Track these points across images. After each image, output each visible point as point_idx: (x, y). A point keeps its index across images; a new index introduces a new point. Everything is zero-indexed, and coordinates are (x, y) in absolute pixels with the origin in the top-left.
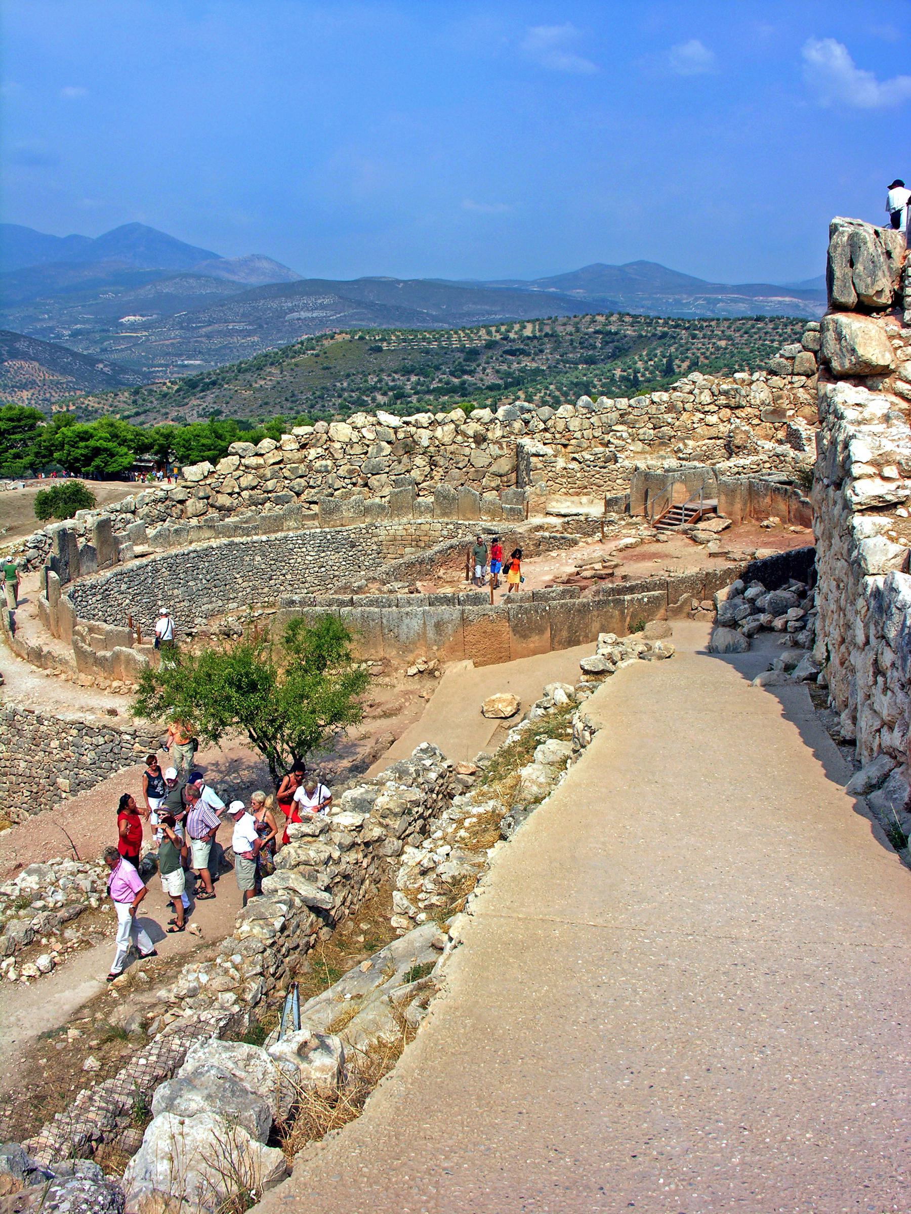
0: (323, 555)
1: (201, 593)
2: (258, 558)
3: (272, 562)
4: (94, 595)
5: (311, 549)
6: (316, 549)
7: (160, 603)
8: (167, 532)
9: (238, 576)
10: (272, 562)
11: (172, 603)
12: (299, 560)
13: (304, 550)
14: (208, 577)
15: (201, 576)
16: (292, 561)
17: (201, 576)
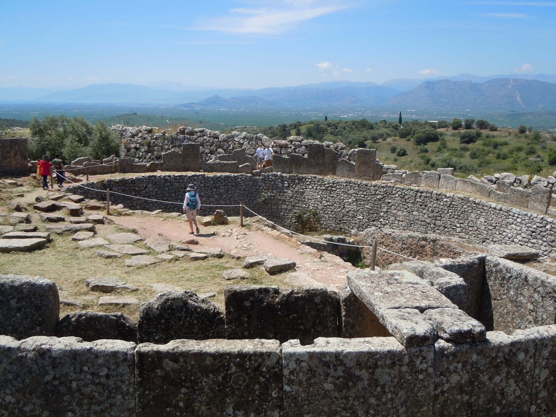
0: (534, 241)
1: (419, 222)
2: (482, 220)
3: (490, 228)
4: (321, 185)
5: (524, 229)
6: (528, 232)
7: (382, 213)
8: (437, 177)
9: (458, 225)
10: (490, 228)
11: (392, 218)
12: (510, 235)
13: (518, 228)
14: (430, 215)
15: (424, 211)
16: (504, 234)
17: (424, 211)
